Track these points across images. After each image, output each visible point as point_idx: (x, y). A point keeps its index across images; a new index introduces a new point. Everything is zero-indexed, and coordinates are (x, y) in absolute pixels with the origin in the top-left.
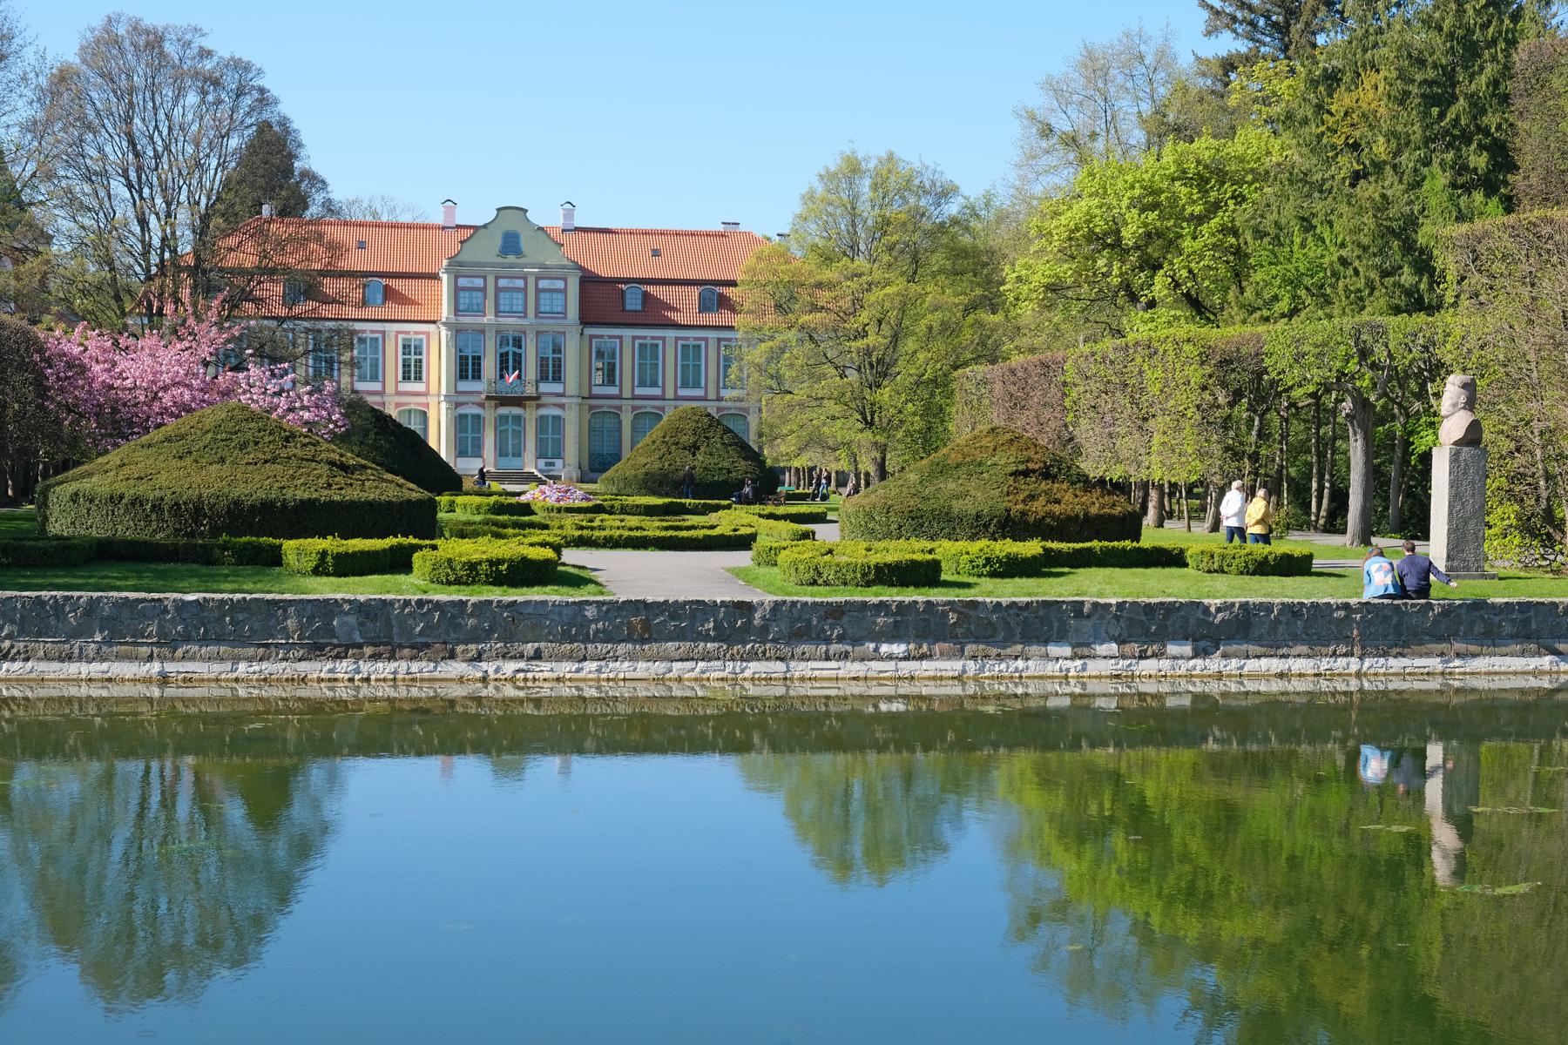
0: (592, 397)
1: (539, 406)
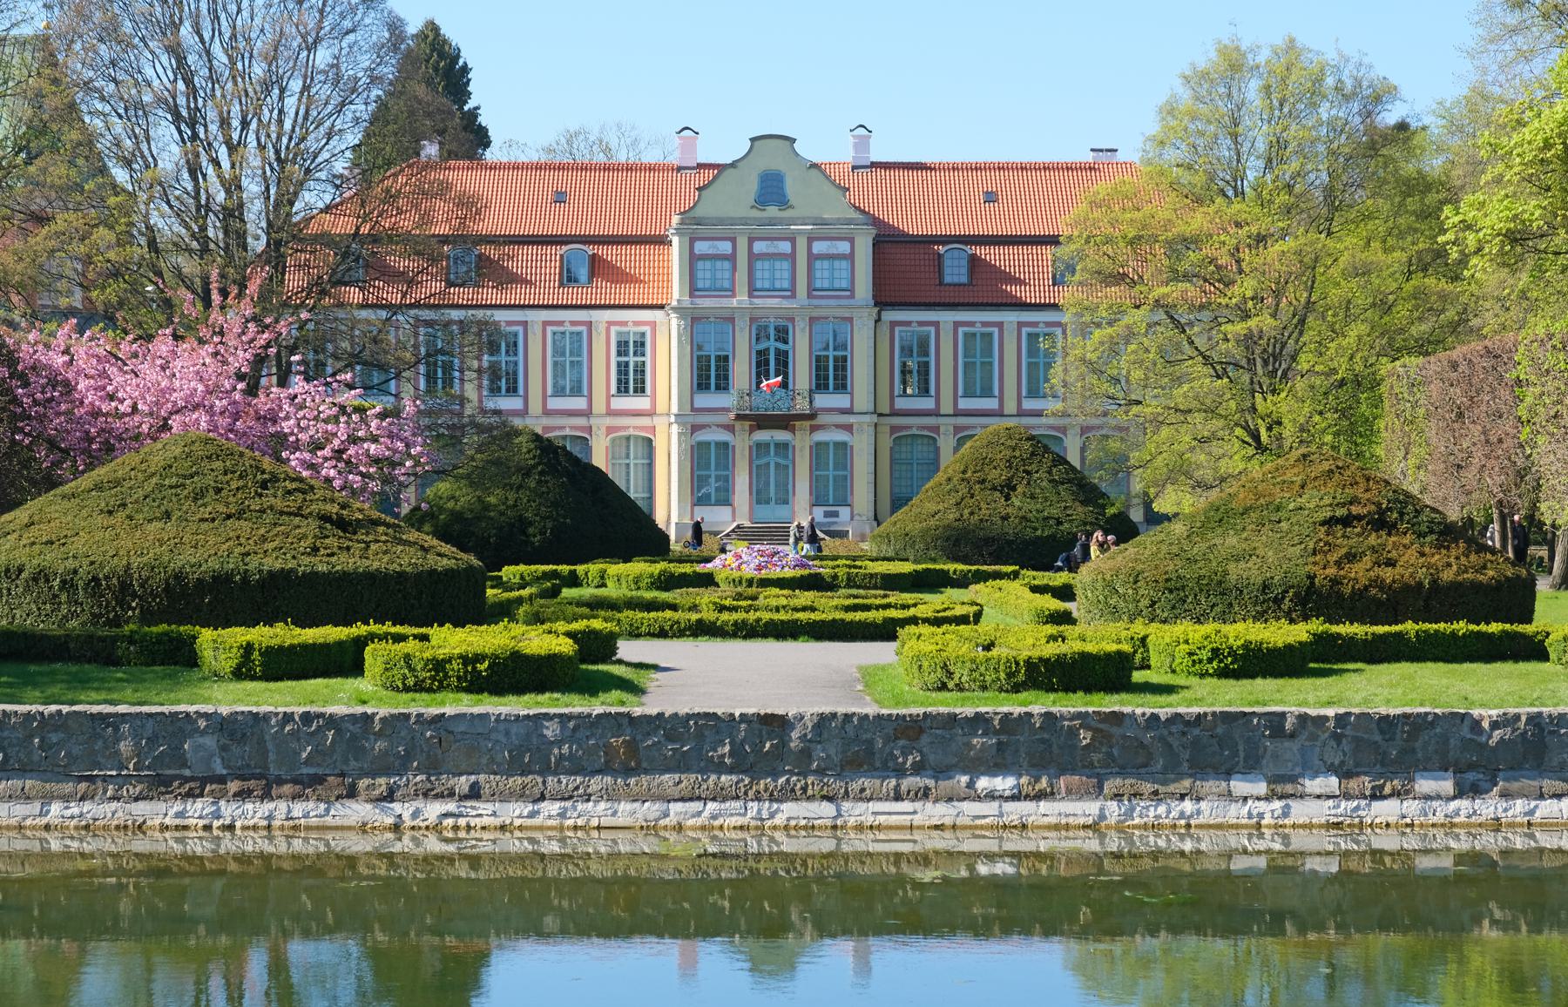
0: (895, 413)
1: (814, 429)
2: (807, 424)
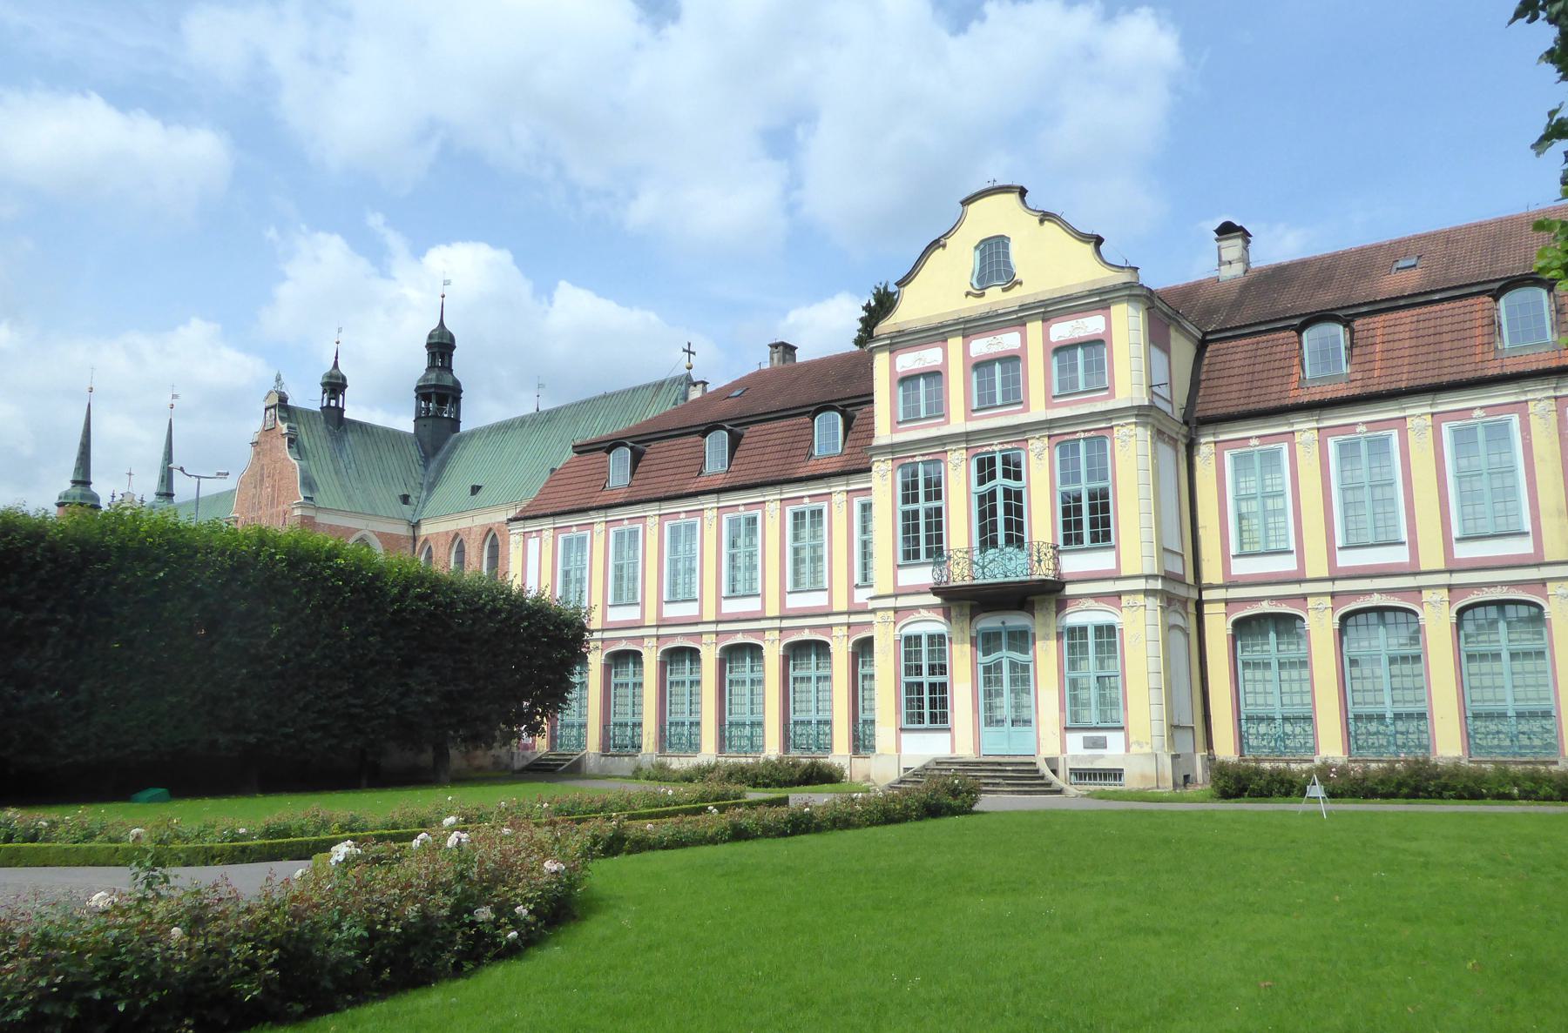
2: (1053, 597)
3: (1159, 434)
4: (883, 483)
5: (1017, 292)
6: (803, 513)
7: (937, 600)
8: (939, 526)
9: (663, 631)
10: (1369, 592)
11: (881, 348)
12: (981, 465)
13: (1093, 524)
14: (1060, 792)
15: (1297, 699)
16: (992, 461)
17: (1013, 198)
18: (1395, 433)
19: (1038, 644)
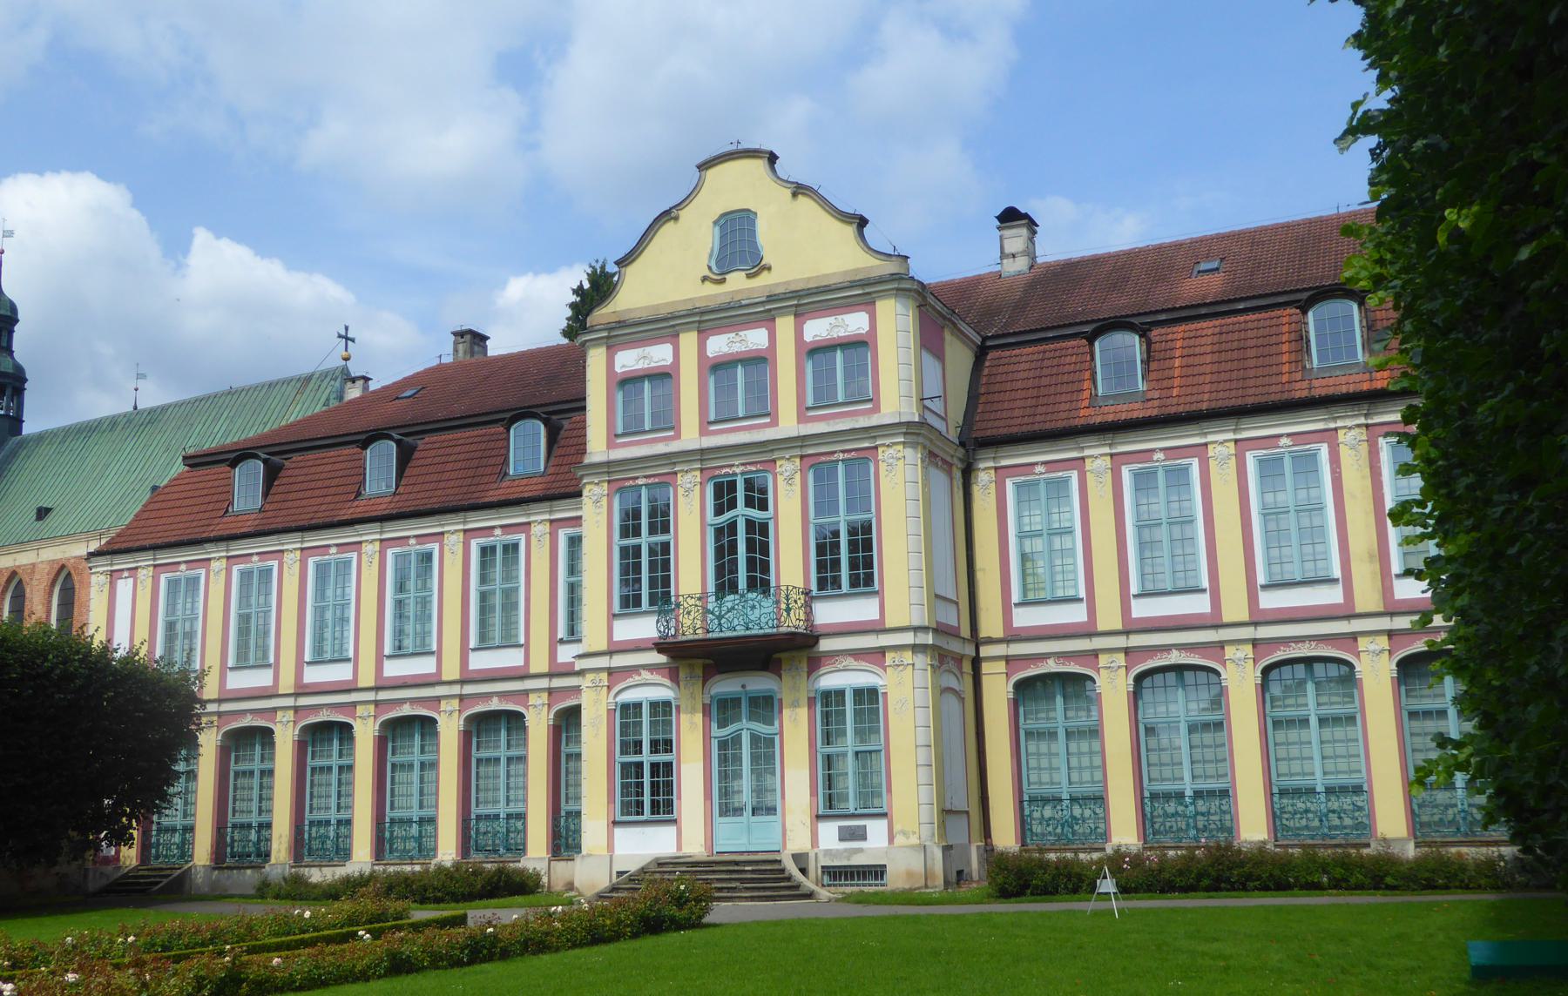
2: (804, 654)
3: (931, 457)
4: (596, 514)
5: (764, 280)
6: (493, 548)
7: (662, 659)
8: (666, 565)
9: (303, 701)
10: (1167, 648)
11: (596, 342)
12: (719, 489)
13: (853, 565)
14: (810, 895)
15: (1086, 776)
16: (732, 486)
17: (760, 165)
18: (1195, 462)
19: (786, 712)
